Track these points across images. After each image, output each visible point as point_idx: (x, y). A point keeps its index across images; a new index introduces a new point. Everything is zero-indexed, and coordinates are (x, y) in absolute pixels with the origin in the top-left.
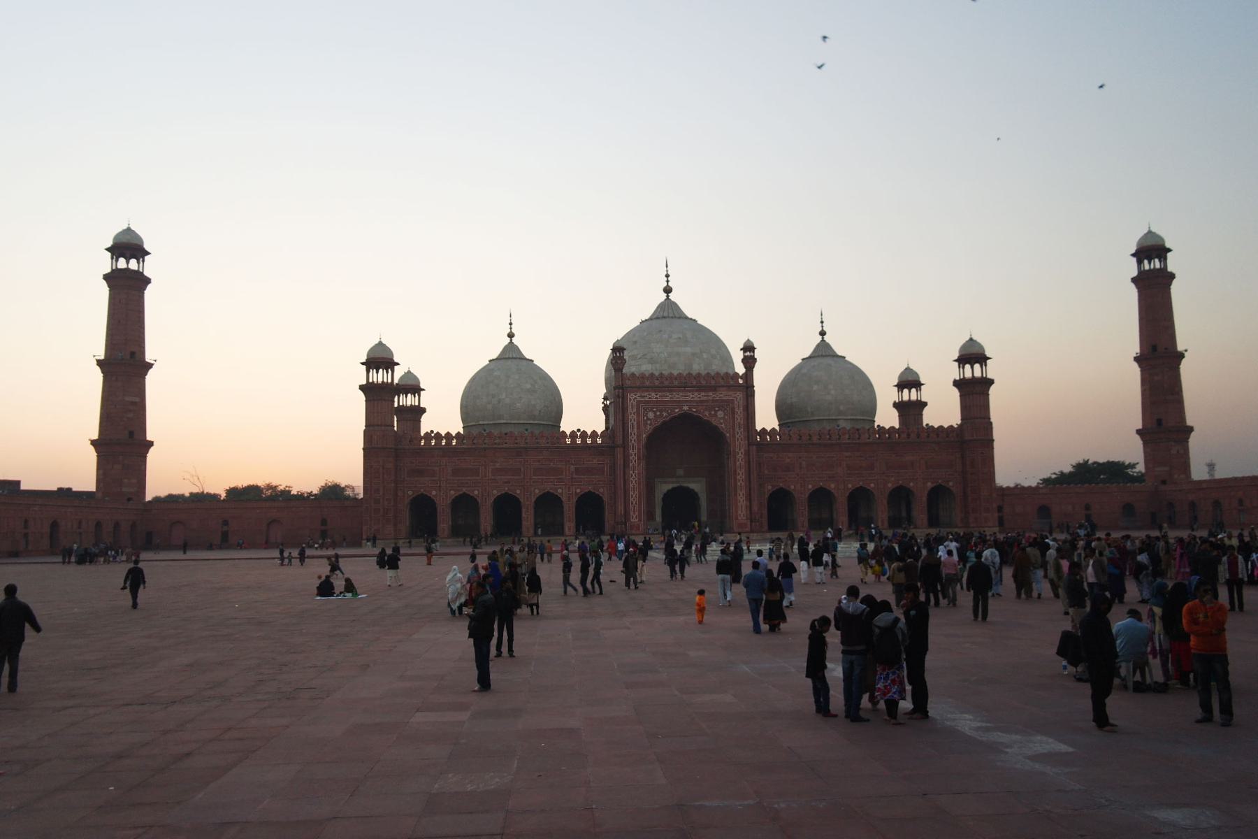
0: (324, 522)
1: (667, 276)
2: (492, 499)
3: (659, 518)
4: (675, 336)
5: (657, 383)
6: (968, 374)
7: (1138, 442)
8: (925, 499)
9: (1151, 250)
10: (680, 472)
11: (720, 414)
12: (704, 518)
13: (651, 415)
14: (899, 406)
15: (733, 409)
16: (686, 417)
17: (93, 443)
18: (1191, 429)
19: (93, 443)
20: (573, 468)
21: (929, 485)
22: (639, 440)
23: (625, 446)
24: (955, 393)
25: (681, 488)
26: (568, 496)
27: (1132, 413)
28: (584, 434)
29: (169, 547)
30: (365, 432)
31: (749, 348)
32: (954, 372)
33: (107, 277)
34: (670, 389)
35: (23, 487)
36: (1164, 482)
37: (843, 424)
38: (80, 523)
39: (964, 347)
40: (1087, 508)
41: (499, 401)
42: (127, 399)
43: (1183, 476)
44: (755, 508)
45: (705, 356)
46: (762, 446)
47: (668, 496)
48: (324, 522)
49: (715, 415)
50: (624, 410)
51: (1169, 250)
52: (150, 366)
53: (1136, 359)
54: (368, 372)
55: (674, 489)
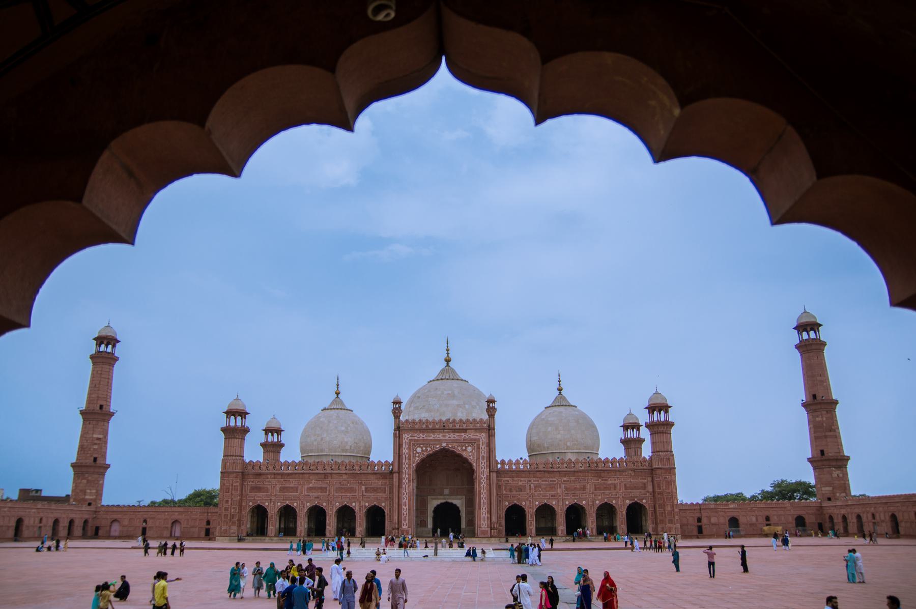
0: (208, 523)
1: (448, 350)
3: (430, 525)
4: (445, 392)
5: (424, 426)
7: (809, 467)
8: (624, 513)
10: (446, 491)
11: (469, 449)
12: (463, 526)
13: (419, 450)
14: (626, 442)
16: (444, 451)
17: (74, 466)
18: (848, 458)
19: (74, 466)
20: (363, 487)
21: (628, 502)
23: (400, 472)
25: (447, 503)
28: (373, 464)
29: (109, 537)
31: (491, 401)
33: (92, 357)
34: (433, 431)
35: (44, 494)
36: (829, 499)
37: (569, 456)
38: (41, 519)
39: (650, 399)
41: (322, 439)
42: (95, 436)
43: (844, 494)
44: (494, 519)
45: (467, 406)
46: (499, 473)
47: (438, 510)
48: (208, 523)
49: (465, 450)
50: (400, 446)
51: (821, 325)
52: (112, 414)
53: (804, 405)
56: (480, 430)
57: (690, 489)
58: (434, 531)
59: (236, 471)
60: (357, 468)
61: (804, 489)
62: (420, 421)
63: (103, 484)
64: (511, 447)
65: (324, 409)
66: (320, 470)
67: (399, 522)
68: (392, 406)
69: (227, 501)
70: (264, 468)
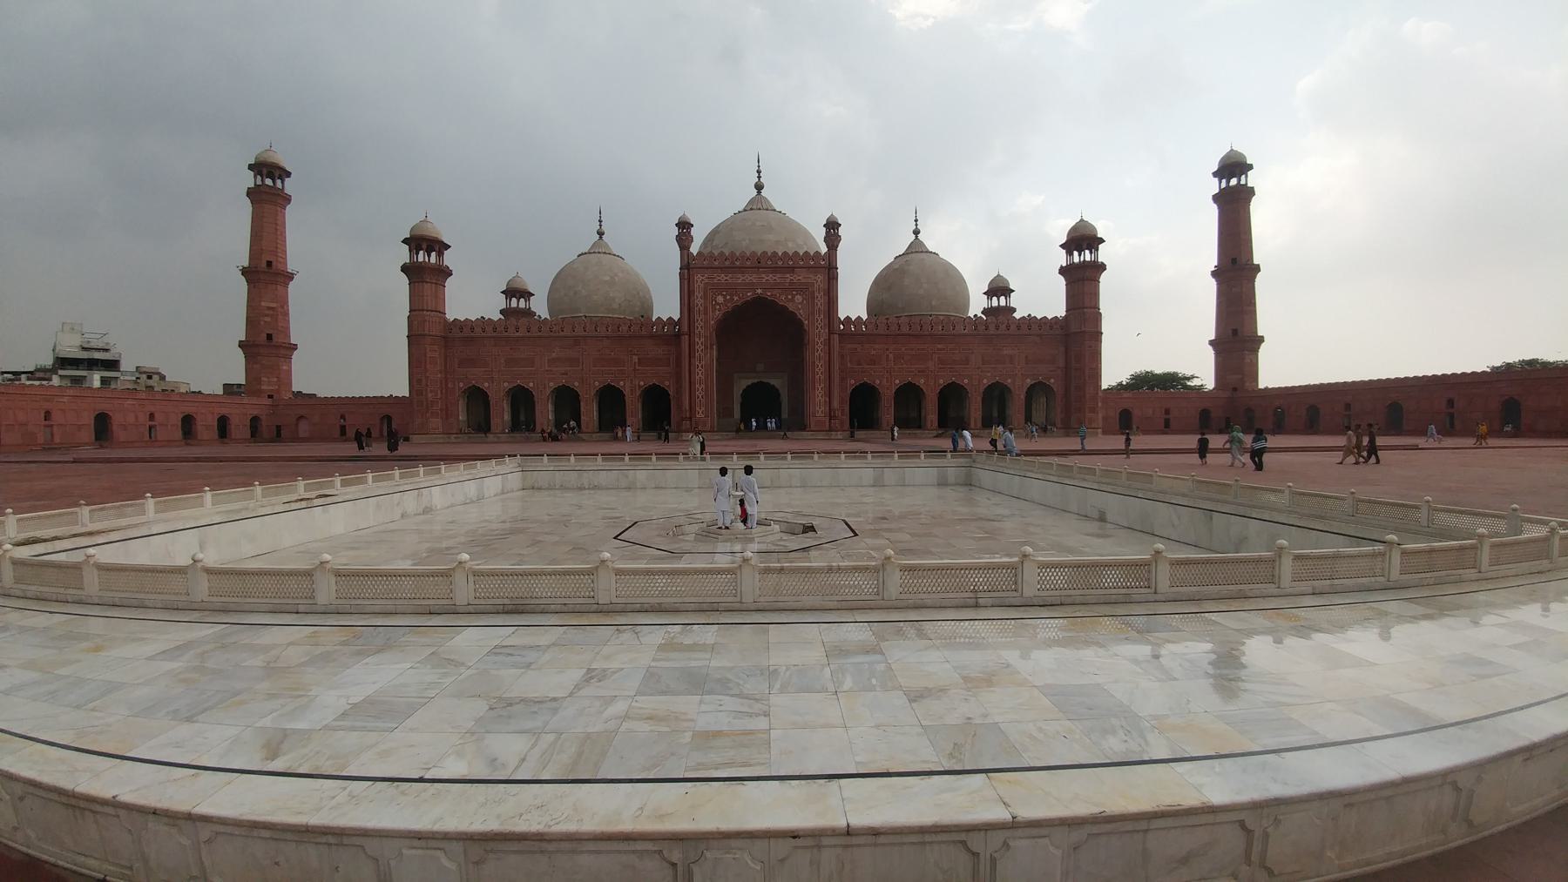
2: (548, 392)
3: (737, 414)
6: (1076, 259)
7: (1209, 355)
9: (1233, 167)
10: (760, 367)
11: (799, 298)
13: (720, 299)
17: (241, 345)
18: (1261, 339)
19: (241, 345)
20: (635, 359)
21: (1029, 382)
24: (1062, 281)
27: (1205, 322)
29: (296, 439)
32: (1061, 258)
34: (742, 269)
38: (152, 416)
40: (1167, 412)
47: (748, 392)
49: (792, 300)
56: (815, 269)
57: (1115, 369)
58: (746, 420)
60: (625, 328)
61: (1171, 381)
62: (722, 254)
63: (290, 371)
68: (676, 231)
69: (419, 381)
70: (478, 330)
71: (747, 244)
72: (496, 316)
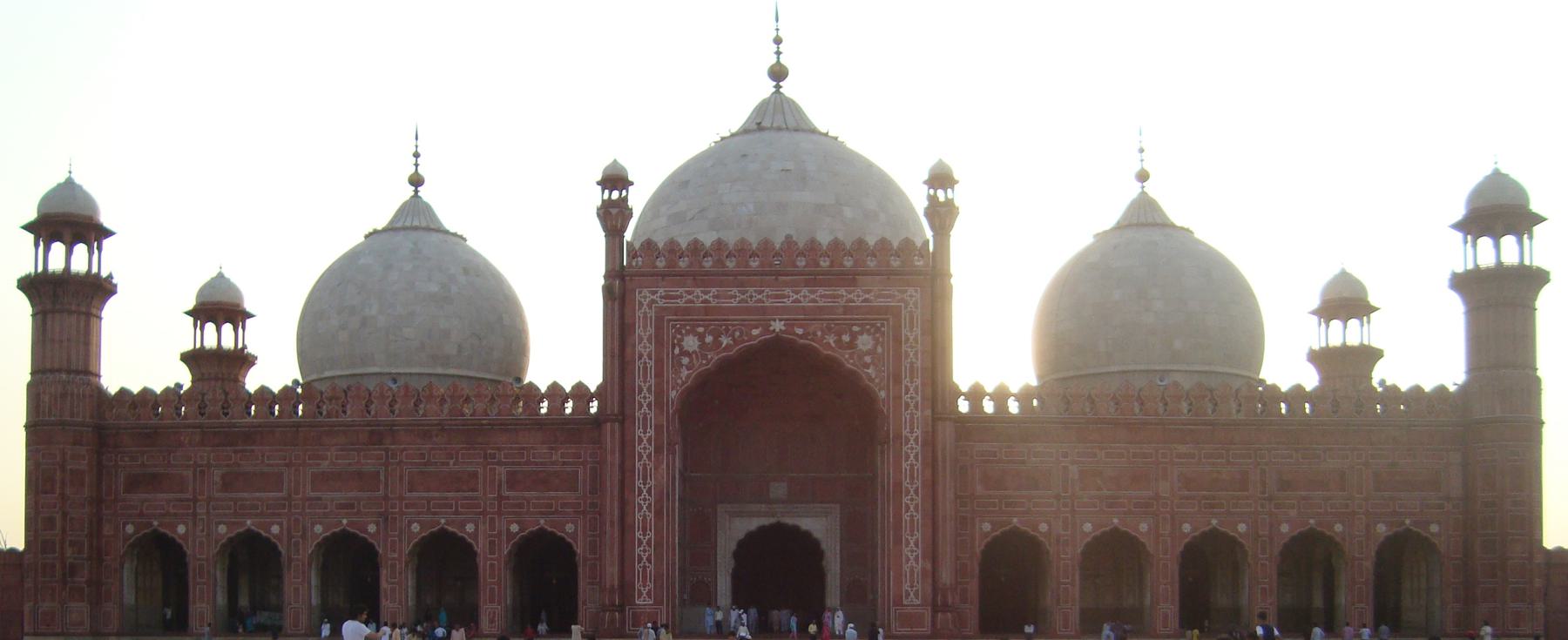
5: (708, 264)
10: (779, 490)
13: (691, 343)
15: (897, 328)
20: (502, 471)
22: (659, 404)
26: (492, 541)
28: (531, 394)
30: (30, 386)
31: (941, 179)
34: (740, 278)
41: (364, 322)
45: (848, 213)
49: (852, 345)
54: (37, 245)
55: (762, 530)
59: (73, 420)
64: (993, 349)
65: (375, 232)
66: (352, 414)
67: (626, 588)
68: (596, 196)
71: (747, 219)
72: (184, 377)
